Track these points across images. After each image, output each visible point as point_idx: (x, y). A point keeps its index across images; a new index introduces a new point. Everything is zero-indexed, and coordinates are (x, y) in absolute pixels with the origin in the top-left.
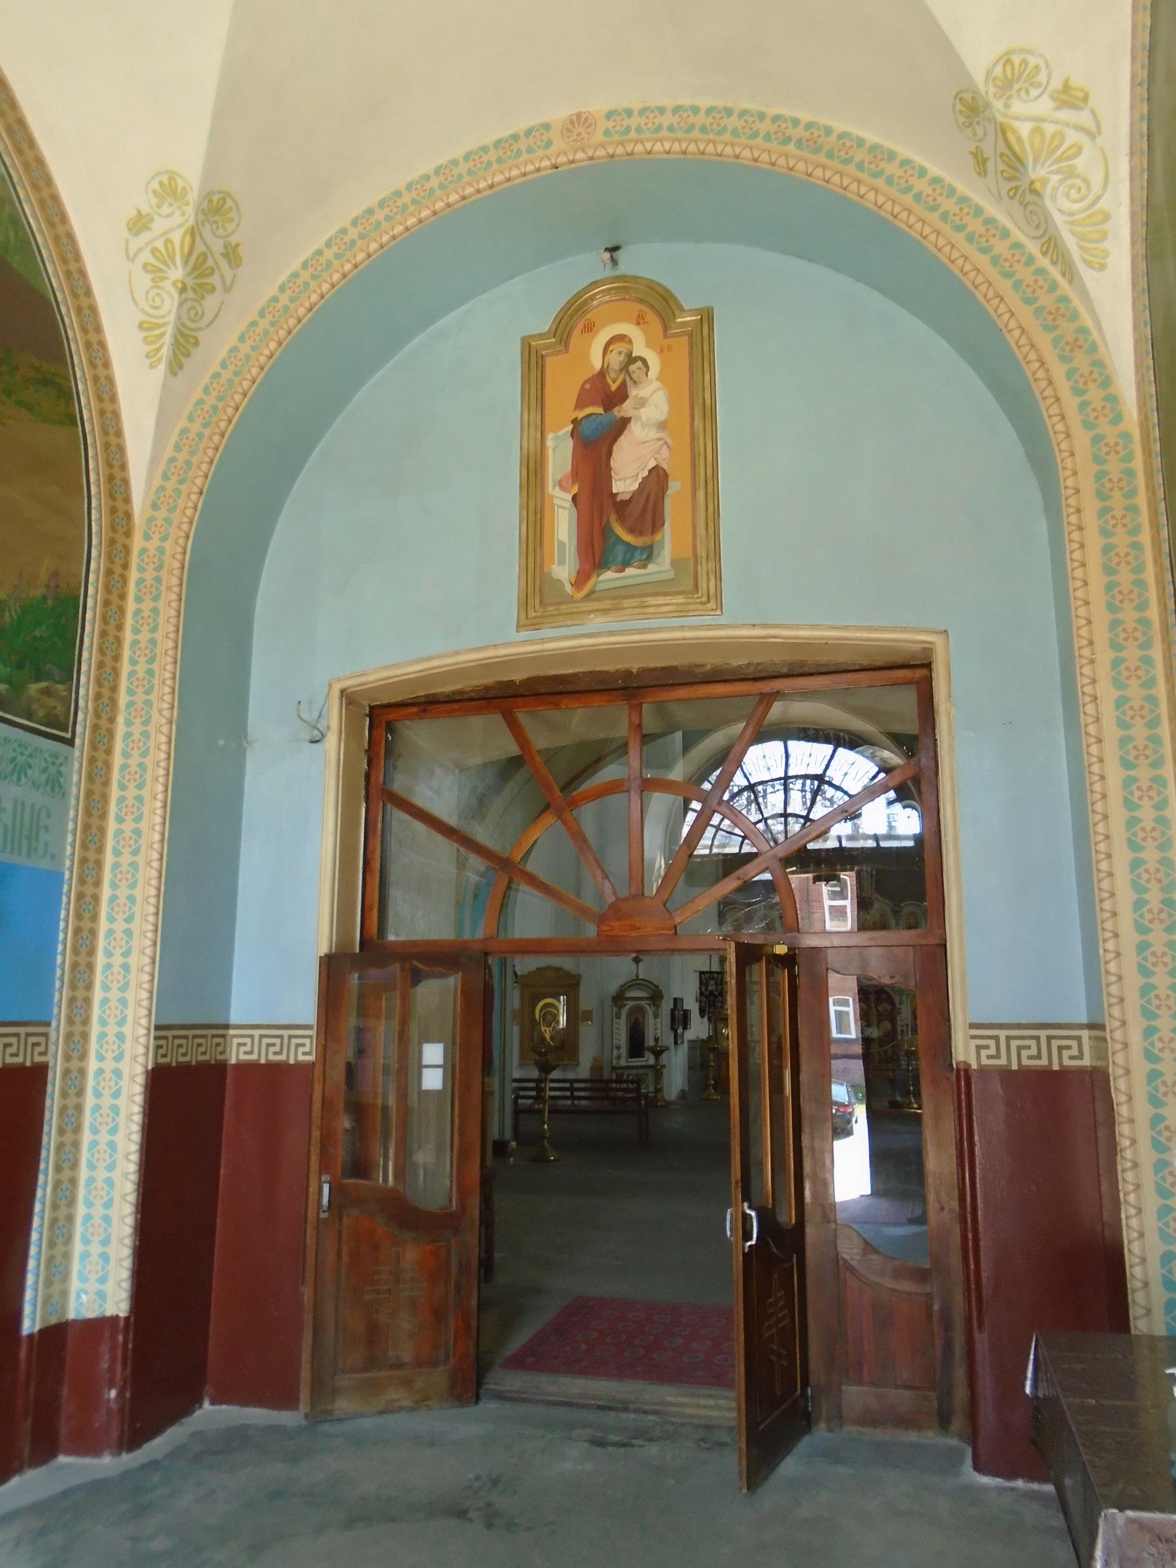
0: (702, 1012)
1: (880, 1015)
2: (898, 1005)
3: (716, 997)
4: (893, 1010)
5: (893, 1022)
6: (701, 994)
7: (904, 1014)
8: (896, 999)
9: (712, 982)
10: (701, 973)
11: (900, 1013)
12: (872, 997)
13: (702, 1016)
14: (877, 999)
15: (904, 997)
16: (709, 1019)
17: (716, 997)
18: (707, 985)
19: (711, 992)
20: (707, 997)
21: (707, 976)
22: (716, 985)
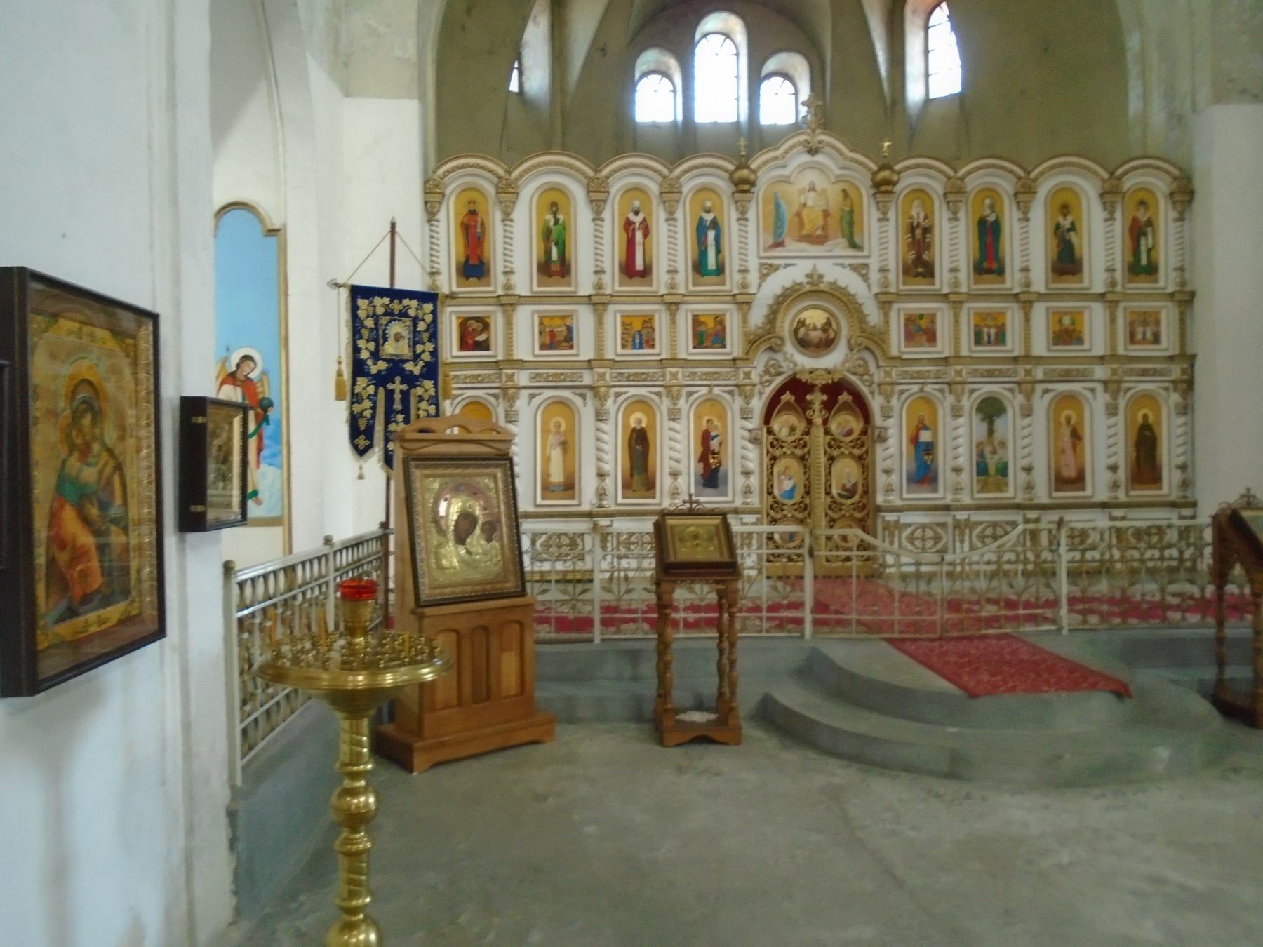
0: (361, 437)
1: (834, 444)
2: (878, 420)
3: (411, 380)
4: (864, 432)
5: (864, 462)
6: (359, 368)
7: (892, 442)
8: (876, 403)
9: (396, 328)
10: (358, 292)
11: (882, 439)
12: (817, 398)
13: (361, 452)
14: (828, 406)
15: (895, 402)
16: (388, 460)
17: (411, 380)
18: (379, 337)
19: (396, 366)
20: (381, 380)
21: (378, 301)
22: (415, 340)
